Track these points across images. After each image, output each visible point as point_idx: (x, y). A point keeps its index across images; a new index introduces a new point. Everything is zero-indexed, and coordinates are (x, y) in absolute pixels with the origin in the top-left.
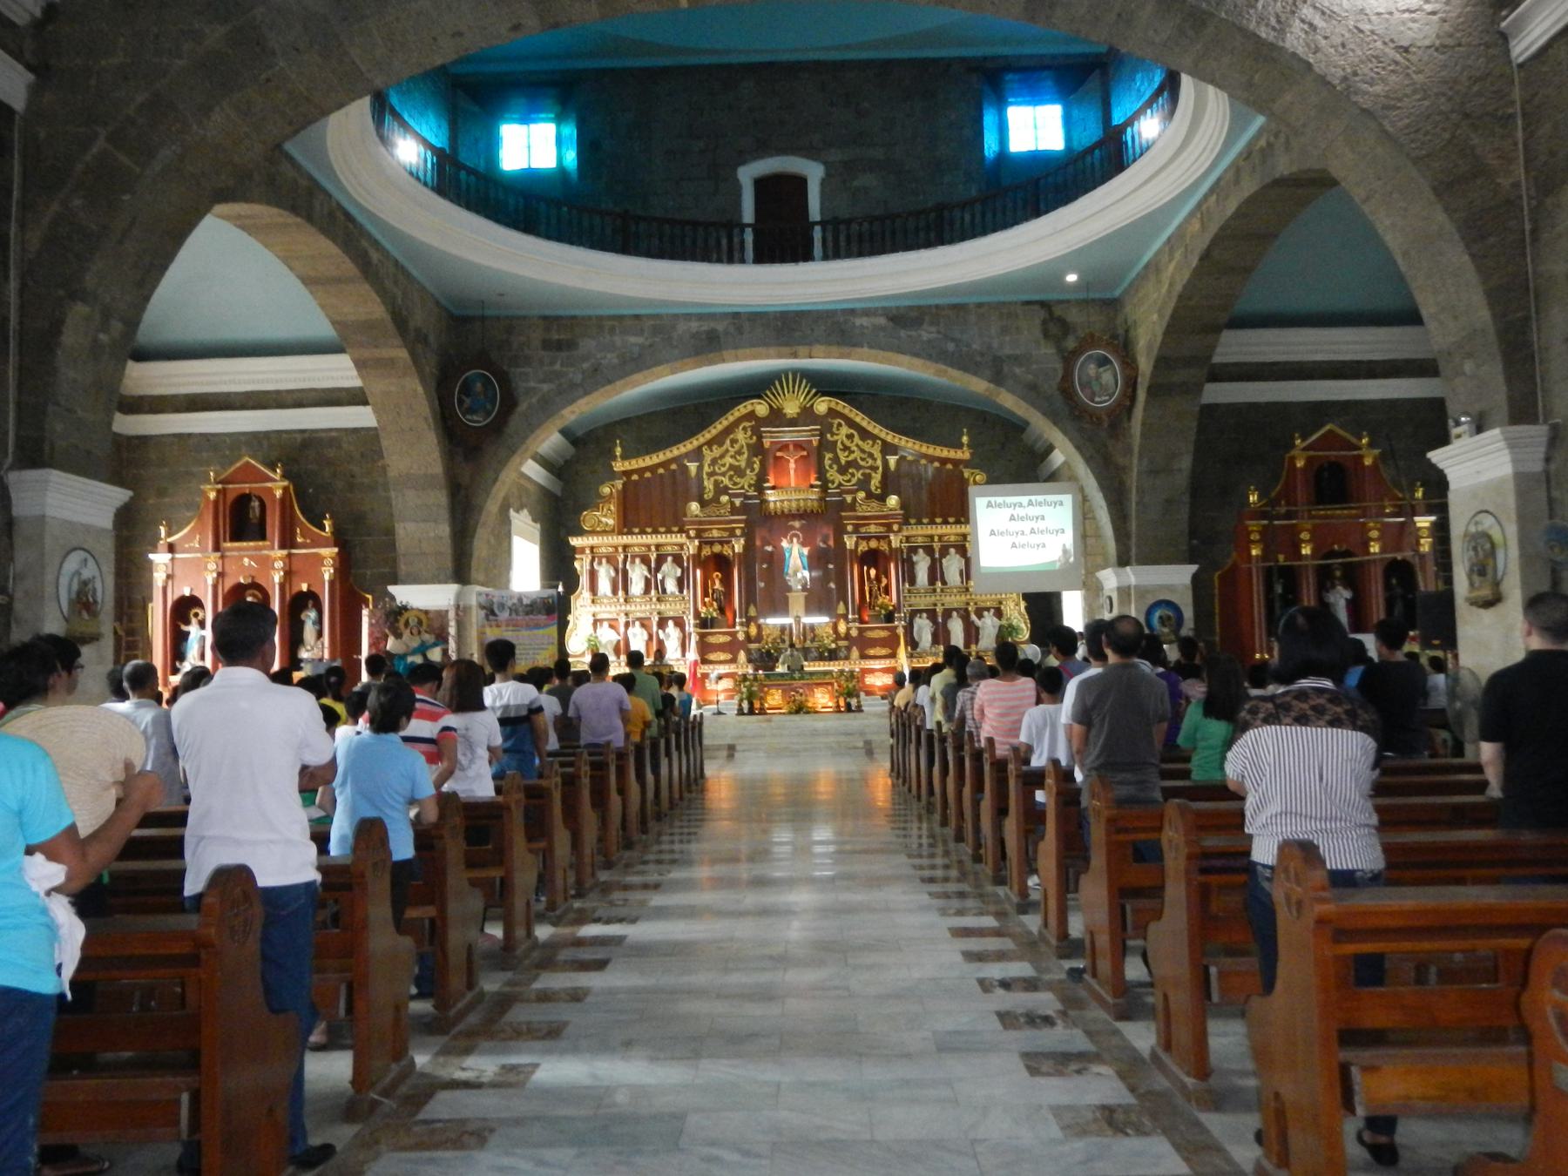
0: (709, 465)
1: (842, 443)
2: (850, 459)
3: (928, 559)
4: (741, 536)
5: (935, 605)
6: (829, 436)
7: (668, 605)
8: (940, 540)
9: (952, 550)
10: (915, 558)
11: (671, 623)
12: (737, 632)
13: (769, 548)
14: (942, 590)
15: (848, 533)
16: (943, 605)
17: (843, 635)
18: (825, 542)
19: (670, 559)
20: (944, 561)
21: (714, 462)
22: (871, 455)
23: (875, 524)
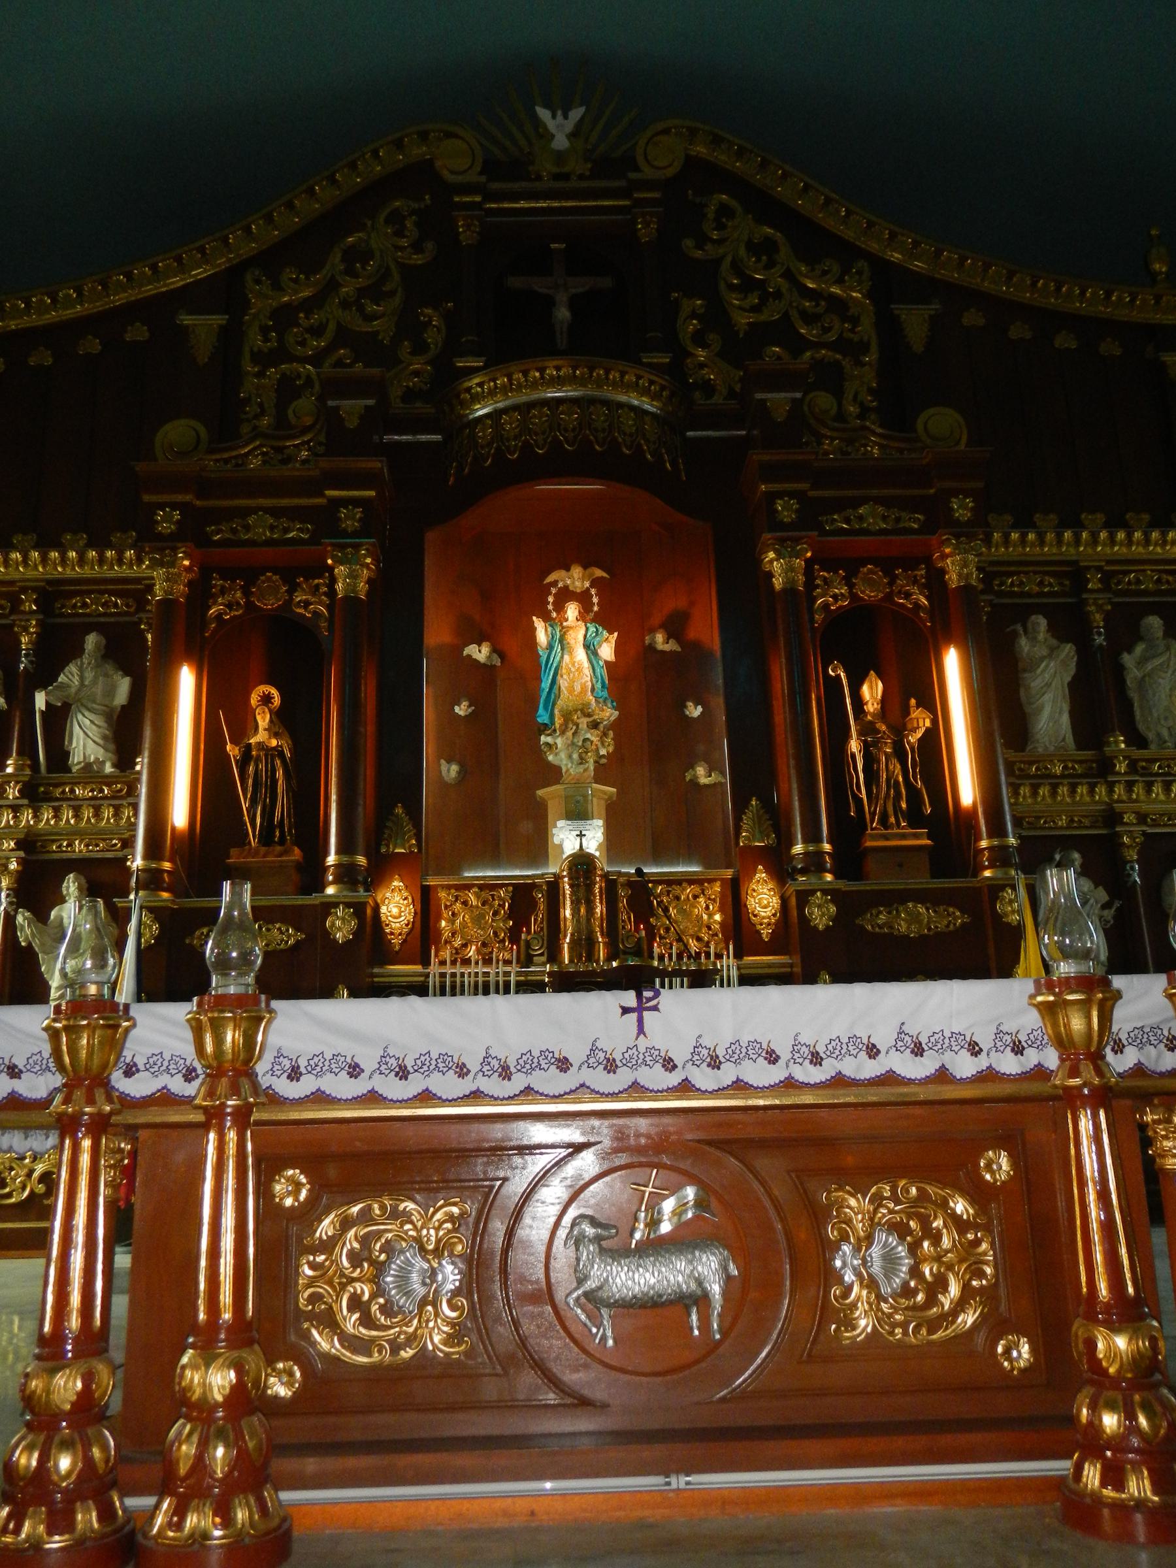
0: (265, 330)
1: (737, 268)
2: (763, 318)
3: (1068, 649)
4: (356, 535)
5: (1111, 817)
6: (688, 243)
7: (68, 814)
8: (1106, 588)
9: (1154, 623)
10: (1024, 644)
11: (71, 886)
12: (328, 907)
13: (480, 653)
14: (1133, 766)
15: (776, 525)
16: (1142, 818)
17: (766, 933)
19: (91, 641)
20: (1127, 659)
21: (284, 317)
22: (839, 306)
23: (878, 501)
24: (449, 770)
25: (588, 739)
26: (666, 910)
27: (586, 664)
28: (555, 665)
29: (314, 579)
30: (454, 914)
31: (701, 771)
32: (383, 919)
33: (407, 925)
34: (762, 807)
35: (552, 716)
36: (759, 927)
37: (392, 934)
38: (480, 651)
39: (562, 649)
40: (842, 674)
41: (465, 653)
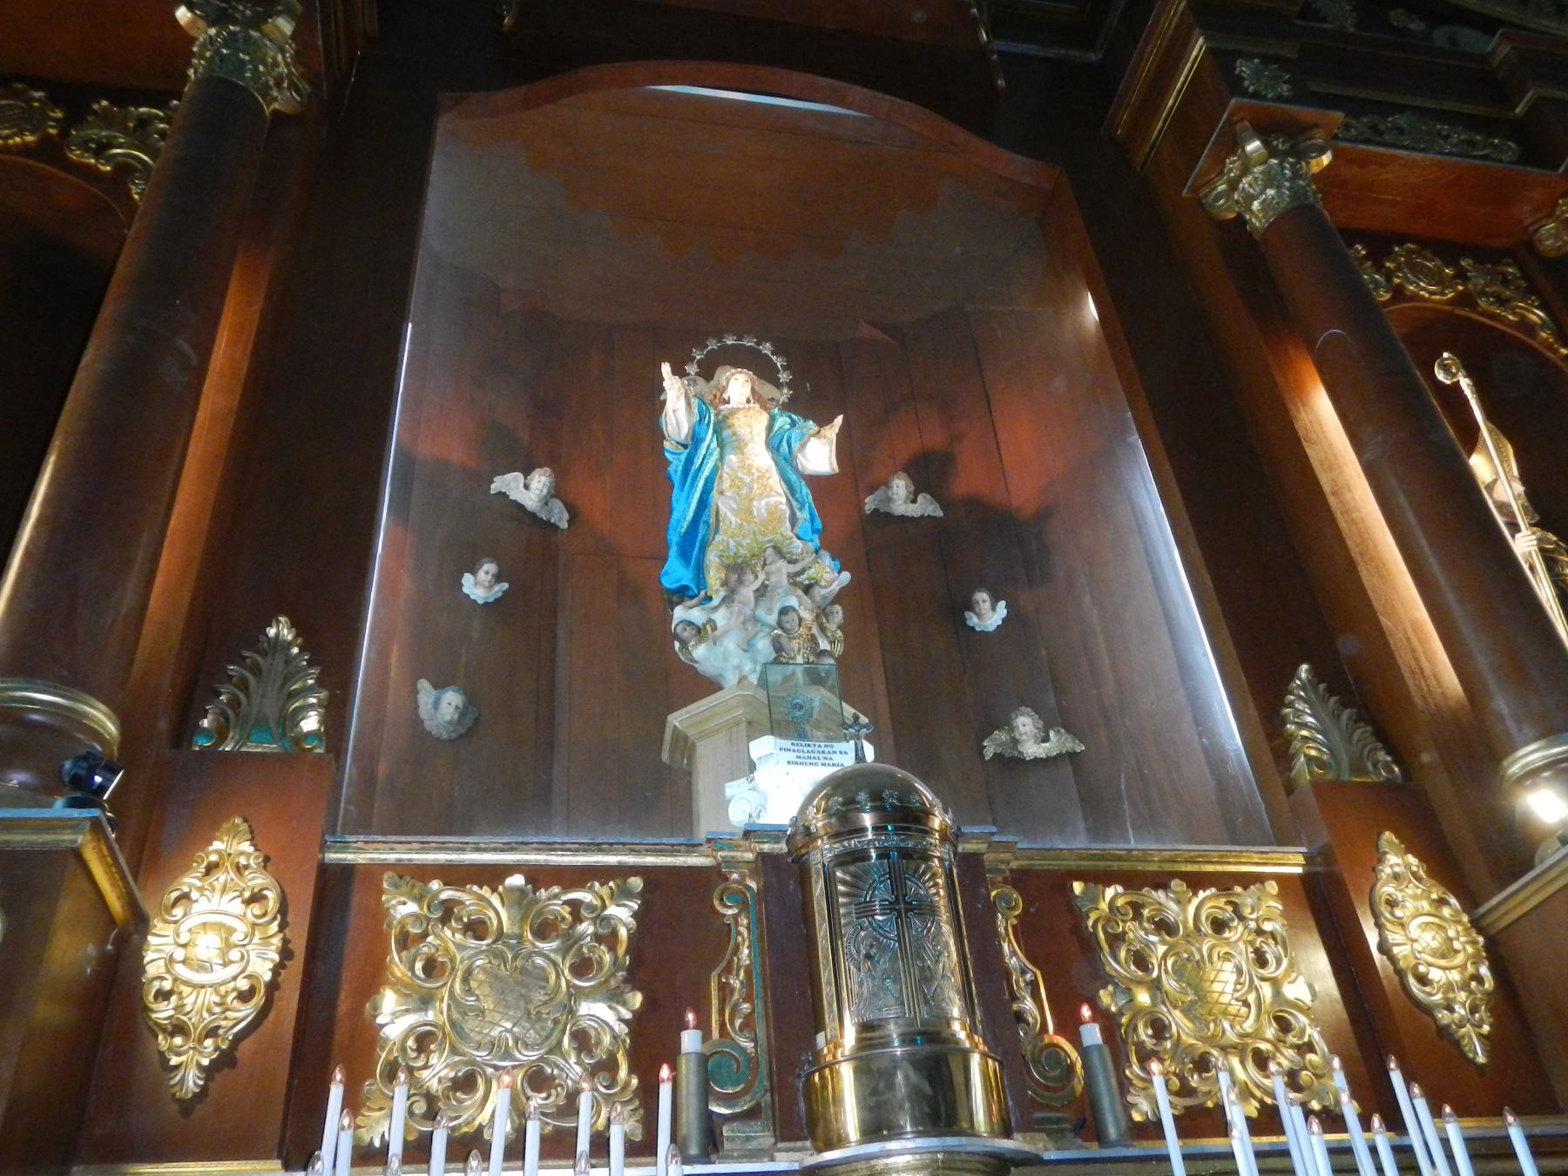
18: (920, 486)
24: (436, 705)
25: (784, 611)
26: (1141, 961)
27: (775, 480)
28: (706, 472)
29: (138, 106)
30: (431, 967)
31: (1025, 723)
32: (152, 970)
33: (244, 997)
34: (1331, 691)
35: (700, 571)
36: (1443, 1016)
37: (179, 1029)
38: (526, 487)
39: (721, 445)
40: (1465, 384)
41: (498, 484)
